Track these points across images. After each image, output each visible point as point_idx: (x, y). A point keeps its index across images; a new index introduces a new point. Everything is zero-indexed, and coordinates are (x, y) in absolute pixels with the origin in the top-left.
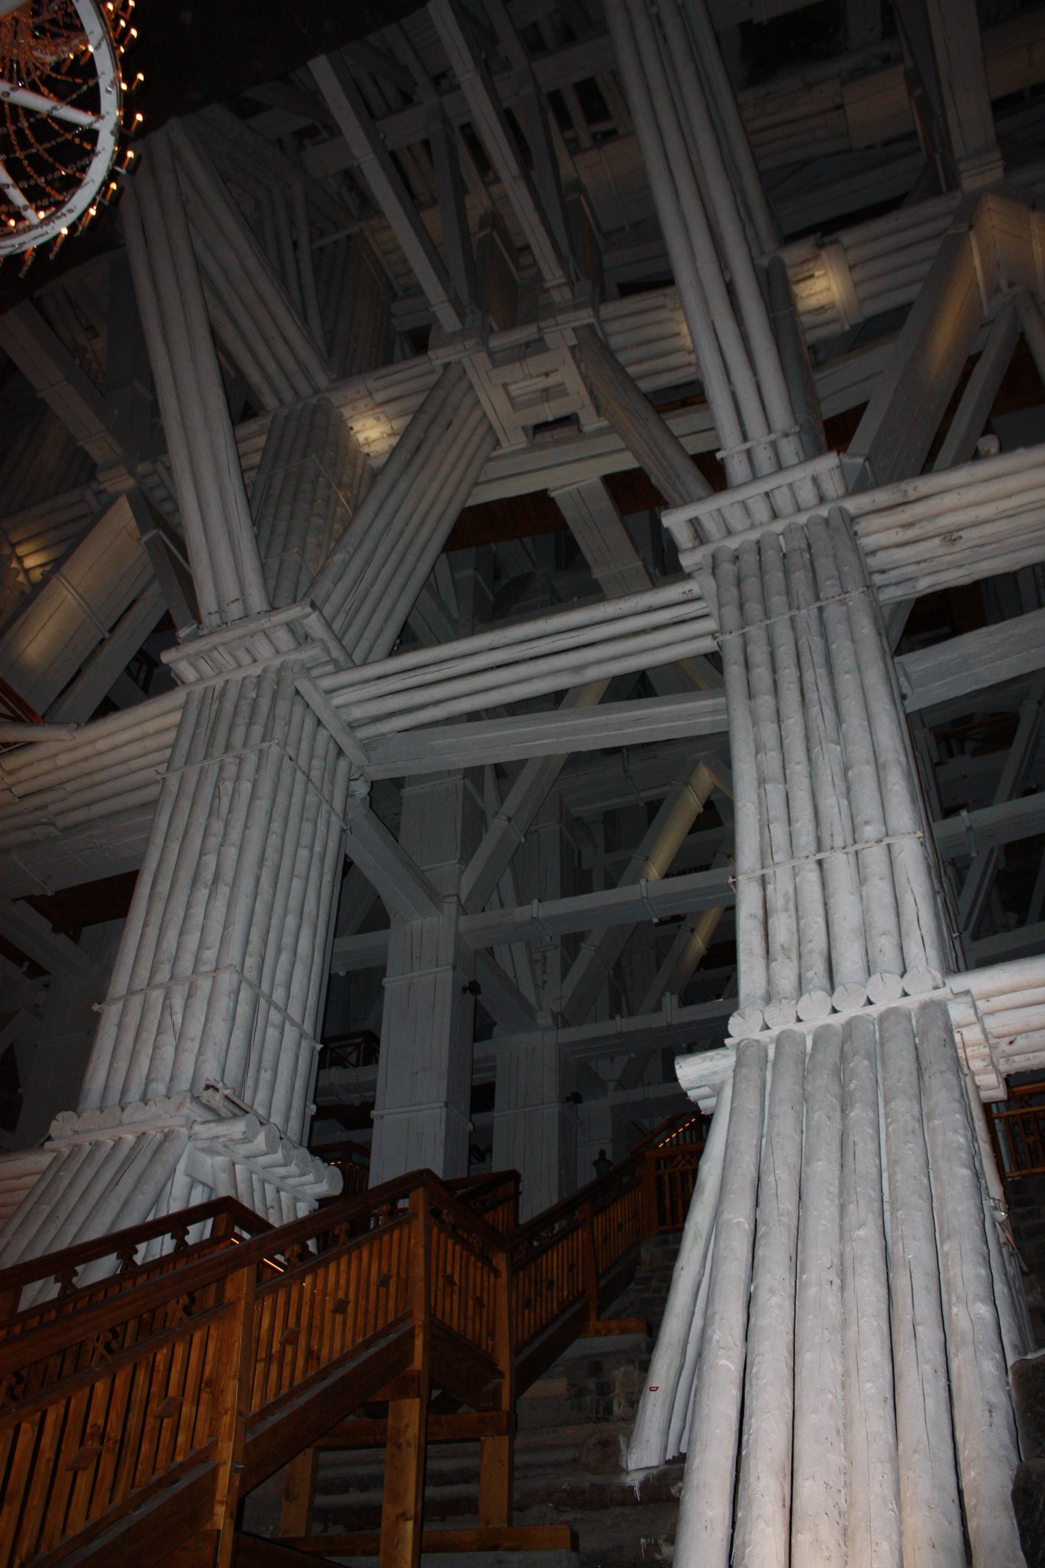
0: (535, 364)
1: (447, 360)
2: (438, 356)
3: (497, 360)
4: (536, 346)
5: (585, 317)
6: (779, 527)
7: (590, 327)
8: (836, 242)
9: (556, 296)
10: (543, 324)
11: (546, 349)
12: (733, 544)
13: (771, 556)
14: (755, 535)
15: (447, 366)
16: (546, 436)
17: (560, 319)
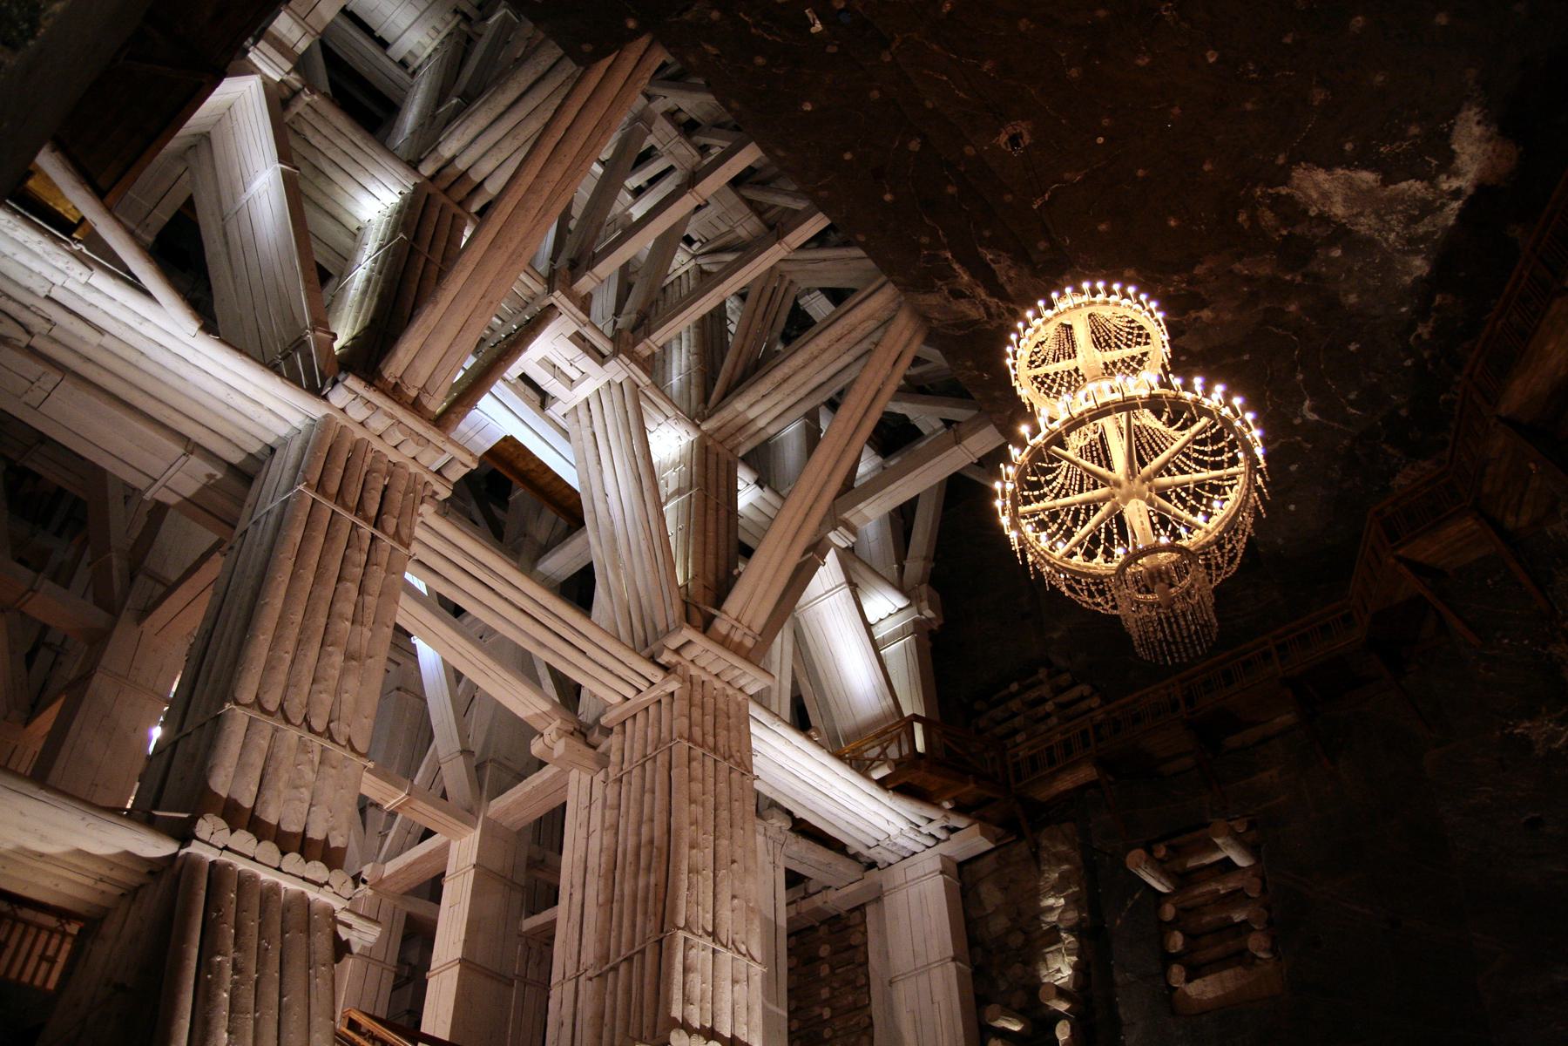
0: (587, 363)
1: (557, 304)
2: (558, 298)
3: (579, 339)
4: (601, 358)
5: (643, 379)
6: (718, 684)
7: (638, 386)
8: (762, 487)
9: (640, 348)
10: (621, 356)
11: (602, 364)
12: (694, 671)
13: (709, 702)
14: (705, 677)
15: (552, 306)
16: (522, 385)
17: (633, 366)
